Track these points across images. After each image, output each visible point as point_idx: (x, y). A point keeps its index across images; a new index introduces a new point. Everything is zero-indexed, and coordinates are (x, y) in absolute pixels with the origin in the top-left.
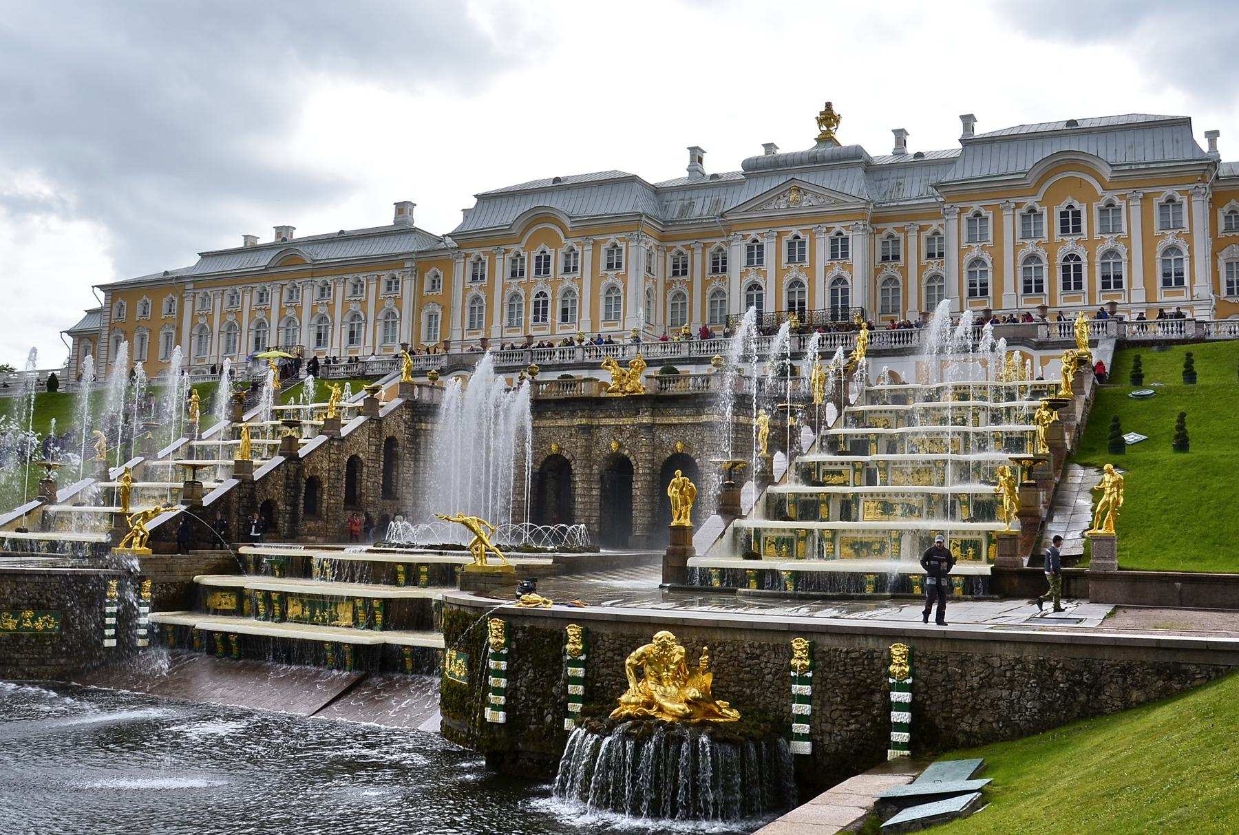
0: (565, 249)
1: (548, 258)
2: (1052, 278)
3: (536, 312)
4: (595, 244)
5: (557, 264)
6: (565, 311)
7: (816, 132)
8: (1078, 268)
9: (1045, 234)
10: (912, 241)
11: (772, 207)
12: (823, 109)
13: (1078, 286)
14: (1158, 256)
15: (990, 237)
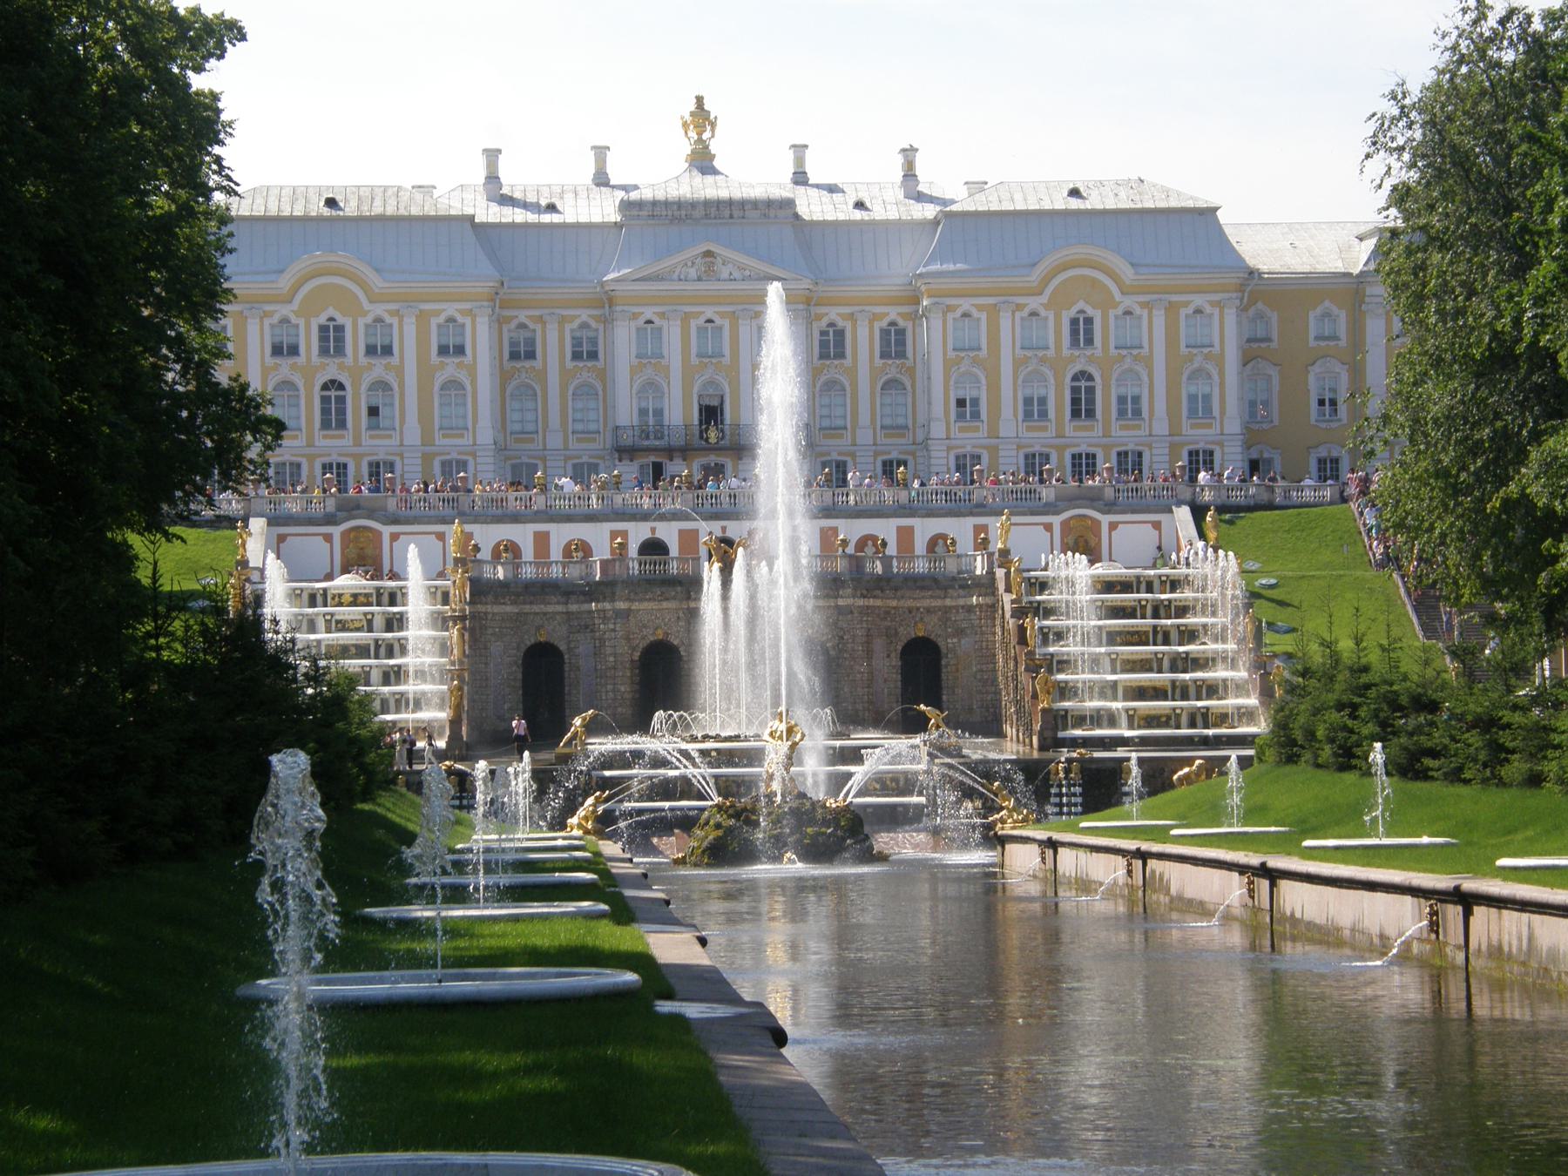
0: (369, 319)
1: (340, 329)
2: (1059, 401)
3: (325, 411)
4: (423, 318)
5: (354, 342)
6: (373, 411)
7: (687, 149)
8: (1091, 391)
9: (1051, 342)
10: (863, 332)
11: (675, 276)
12: (692, 107)
13: (1091, 413)
14: (1184, 377)
15: (984, 345)
